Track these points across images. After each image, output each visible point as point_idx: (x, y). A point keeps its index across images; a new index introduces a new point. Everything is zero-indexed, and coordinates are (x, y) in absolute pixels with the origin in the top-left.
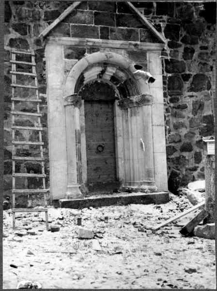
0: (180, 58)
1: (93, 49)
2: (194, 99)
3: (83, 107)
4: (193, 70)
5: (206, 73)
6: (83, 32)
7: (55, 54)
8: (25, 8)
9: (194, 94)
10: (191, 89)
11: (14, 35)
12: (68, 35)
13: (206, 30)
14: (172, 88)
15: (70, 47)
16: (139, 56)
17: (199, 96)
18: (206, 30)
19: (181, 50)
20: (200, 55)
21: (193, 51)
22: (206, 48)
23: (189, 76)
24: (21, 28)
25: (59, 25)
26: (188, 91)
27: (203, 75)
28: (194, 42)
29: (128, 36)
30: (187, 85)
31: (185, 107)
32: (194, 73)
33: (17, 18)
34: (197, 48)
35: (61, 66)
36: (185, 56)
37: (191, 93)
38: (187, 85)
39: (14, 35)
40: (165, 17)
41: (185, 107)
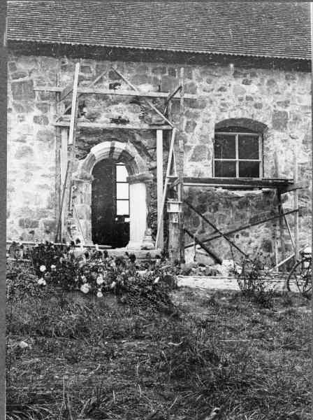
2: (193, 169)
5: (207, 145)
9: (195, 163)
10: (193, 159)
13: (209, 104)
18: (209, 104)
22: (208, 122)
23: (189, 148)
26: (189, 161)
27: (205, 147)
28: (196, 116)
30: (190, 154)
32: (194, 146)
33: (39, 98)
34: (199, 122)
37: (191, 163)
38: (190, 154)
39: (37, 112)
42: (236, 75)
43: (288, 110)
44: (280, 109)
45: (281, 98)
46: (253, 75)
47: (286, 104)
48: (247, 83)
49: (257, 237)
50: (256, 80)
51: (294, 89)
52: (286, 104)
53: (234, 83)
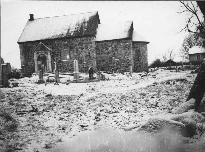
0: (54, 52)
1: (40, 53)
3: (41, 61)
4: (56, 53)
6: (38, 51)
7: (35, 54)
8: (32, 48)
10: (56, 56)
11: (31, 52)
12: (36, 51)
14: (52, 57)
15: (36, 53)
16: (47, 53)
17: (57, 57)
19: (54, 51)
20: (58, 51)
21: (56, 50)
23: (55, 54)
24: (32, 51)
25: (35, 50)
29: (44, 50)
31: (55, 59)
34: (57, 50)
35: (36, 56)
36: (55, 51)
38: (55, 56)
40: (51, 46)
41: (55, 59)
42: (63, 41)
43: (73, 46)
44: (71, 45)
45: (72, 43)
46: (66, 40)
47: (72, 44)
48: (65, 42)
49: (68, 69)
50: (66, 41)
51: (74, 42)
52: (72, 44)
53: (62, 42)
